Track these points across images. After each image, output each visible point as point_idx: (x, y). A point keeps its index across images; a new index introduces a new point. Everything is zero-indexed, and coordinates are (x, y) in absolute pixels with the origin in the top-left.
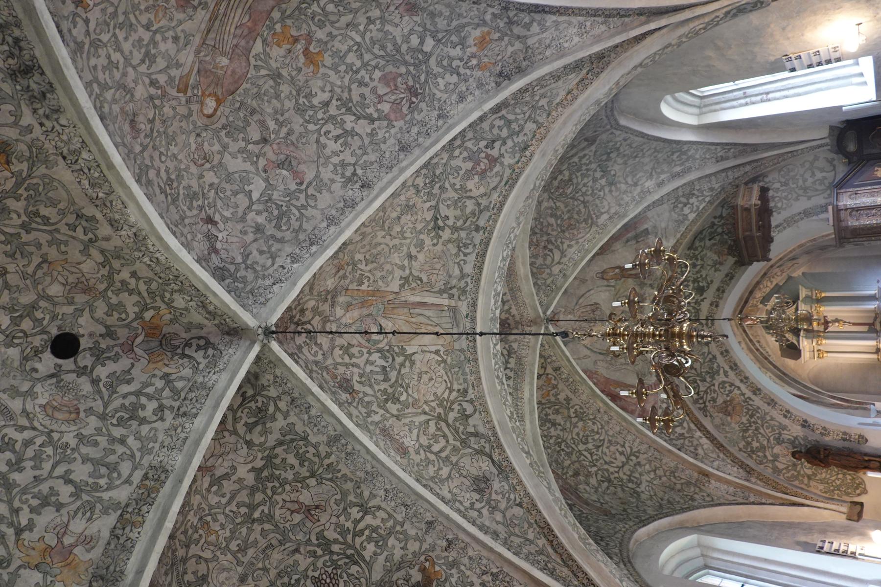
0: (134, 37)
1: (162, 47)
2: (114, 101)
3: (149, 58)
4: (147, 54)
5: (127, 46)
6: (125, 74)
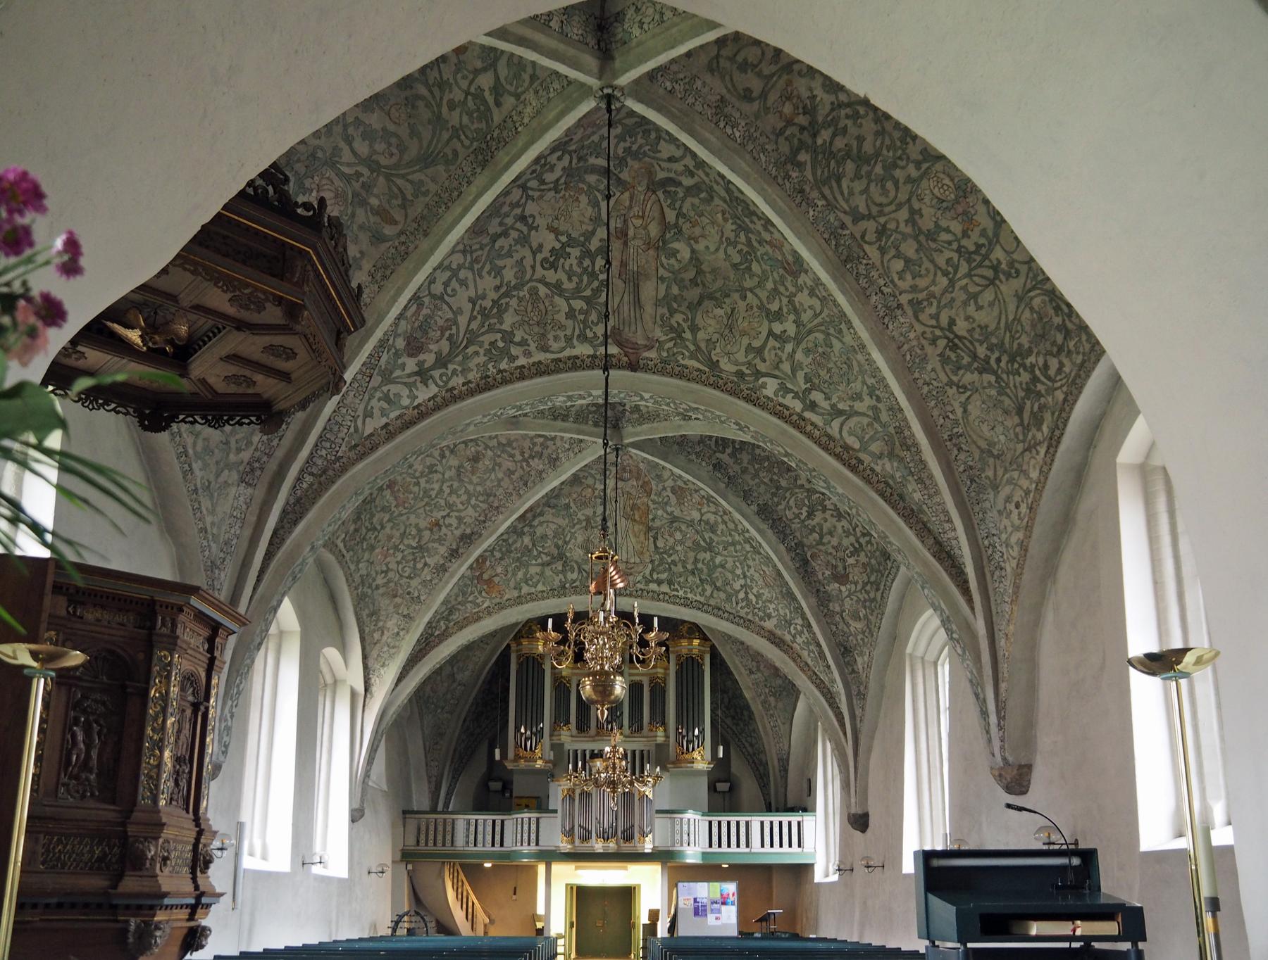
0: (428, 486)
1: (420, 468)
2: (471, 482)
3: (432, 469)
4: (431, 472)
5: (436, 486)
6: (451, 479)
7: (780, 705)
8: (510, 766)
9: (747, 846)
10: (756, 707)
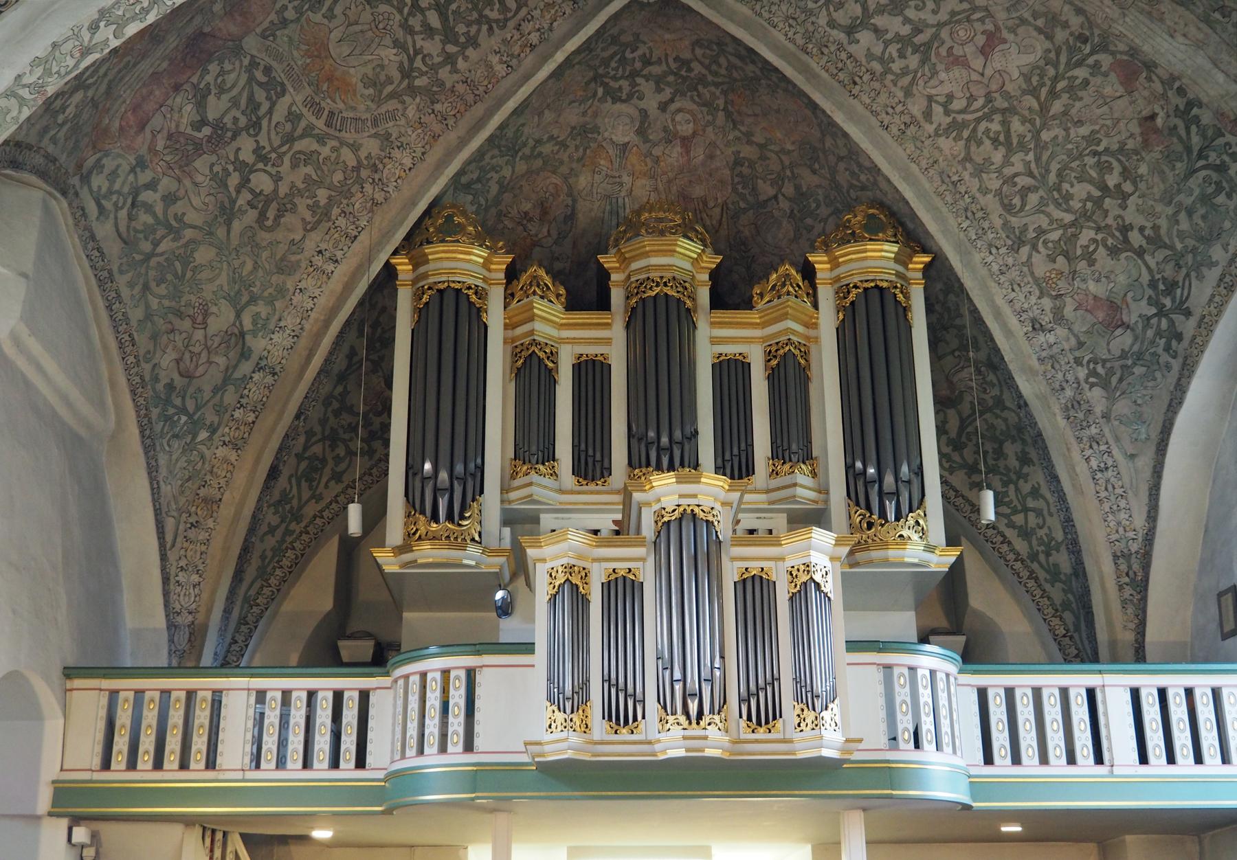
7: (1123, 407)
8: (389, 562)
9: (1099, 760)
10: (1051, 421)
